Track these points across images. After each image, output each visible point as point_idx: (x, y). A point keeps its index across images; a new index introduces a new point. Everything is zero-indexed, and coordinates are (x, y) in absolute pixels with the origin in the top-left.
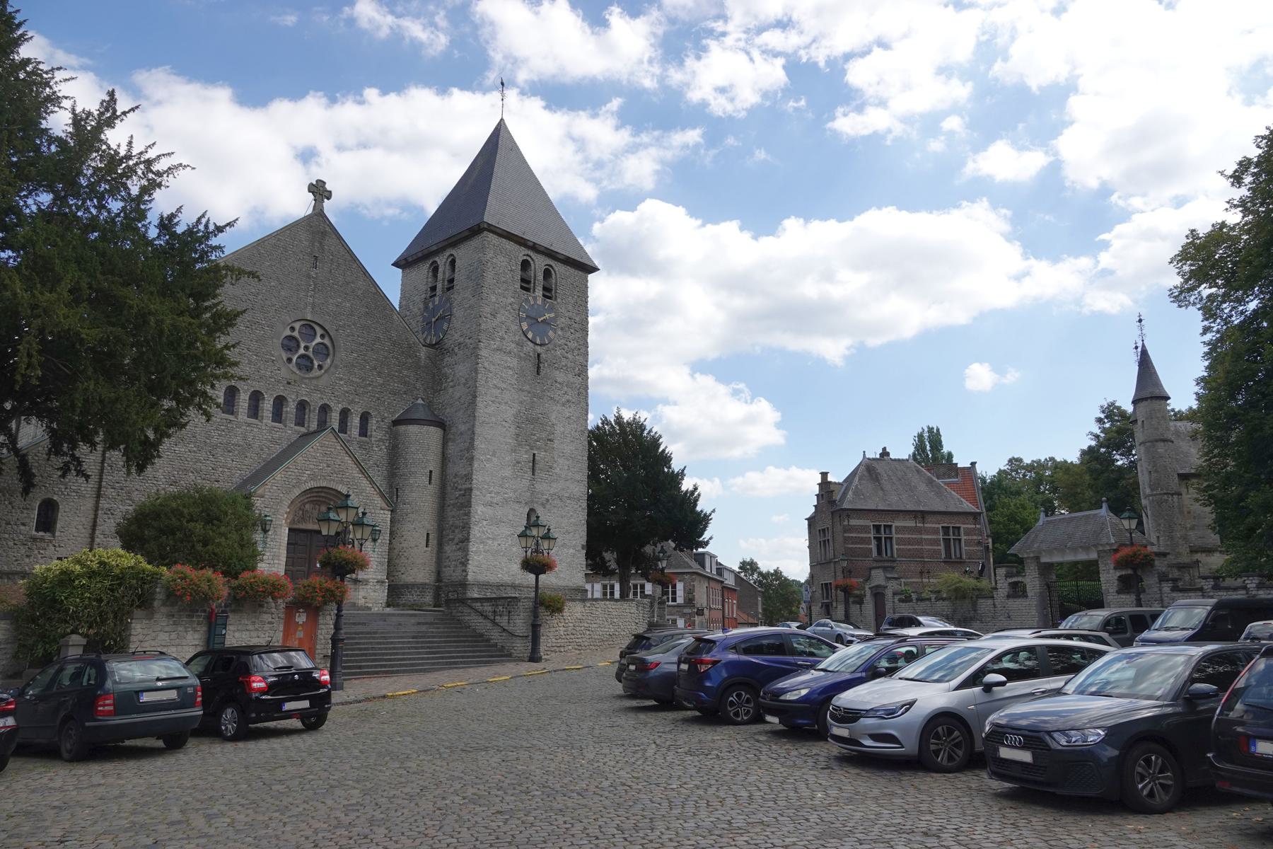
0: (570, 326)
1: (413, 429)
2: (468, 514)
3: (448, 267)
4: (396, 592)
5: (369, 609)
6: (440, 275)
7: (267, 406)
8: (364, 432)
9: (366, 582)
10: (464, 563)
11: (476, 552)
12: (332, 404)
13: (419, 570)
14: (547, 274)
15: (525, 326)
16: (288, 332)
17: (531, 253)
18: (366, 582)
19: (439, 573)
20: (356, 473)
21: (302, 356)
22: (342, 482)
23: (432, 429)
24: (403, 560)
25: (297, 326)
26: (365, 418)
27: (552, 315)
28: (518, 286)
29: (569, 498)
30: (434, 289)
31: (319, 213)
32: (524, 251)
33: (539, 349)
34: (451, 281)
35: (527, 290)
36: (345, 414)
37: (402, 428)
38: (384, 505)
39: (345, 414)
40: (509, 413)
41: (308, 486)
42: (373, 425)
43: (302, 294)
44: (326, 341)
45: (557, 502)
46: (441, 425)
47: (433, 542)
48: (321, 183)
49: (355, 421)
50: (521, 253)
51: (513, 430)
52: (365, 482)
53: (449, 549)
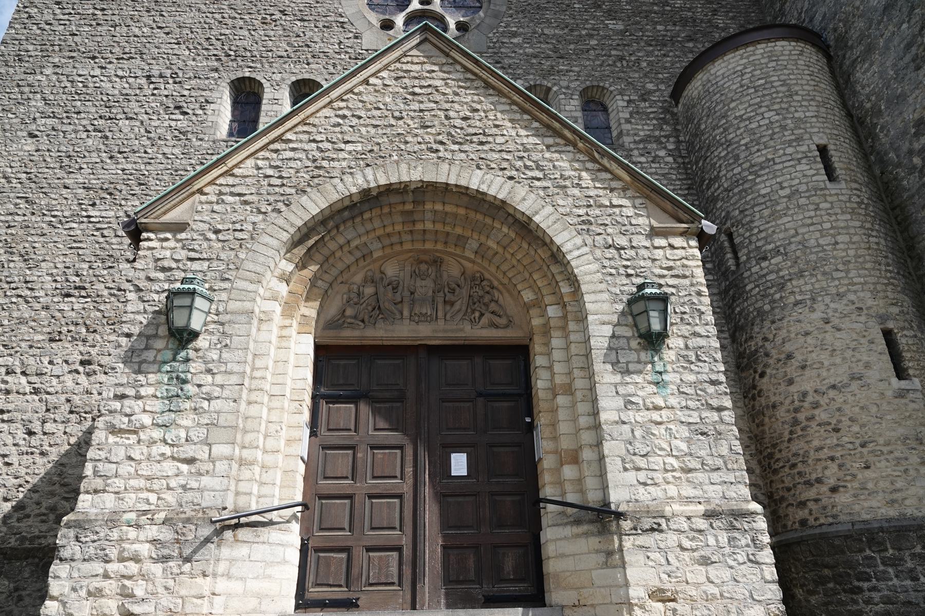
1: (724, 67)
9: (654, 523)
24: (817, 437)
37: (695, 87)
41: (354, 184)
42: (619, 107)
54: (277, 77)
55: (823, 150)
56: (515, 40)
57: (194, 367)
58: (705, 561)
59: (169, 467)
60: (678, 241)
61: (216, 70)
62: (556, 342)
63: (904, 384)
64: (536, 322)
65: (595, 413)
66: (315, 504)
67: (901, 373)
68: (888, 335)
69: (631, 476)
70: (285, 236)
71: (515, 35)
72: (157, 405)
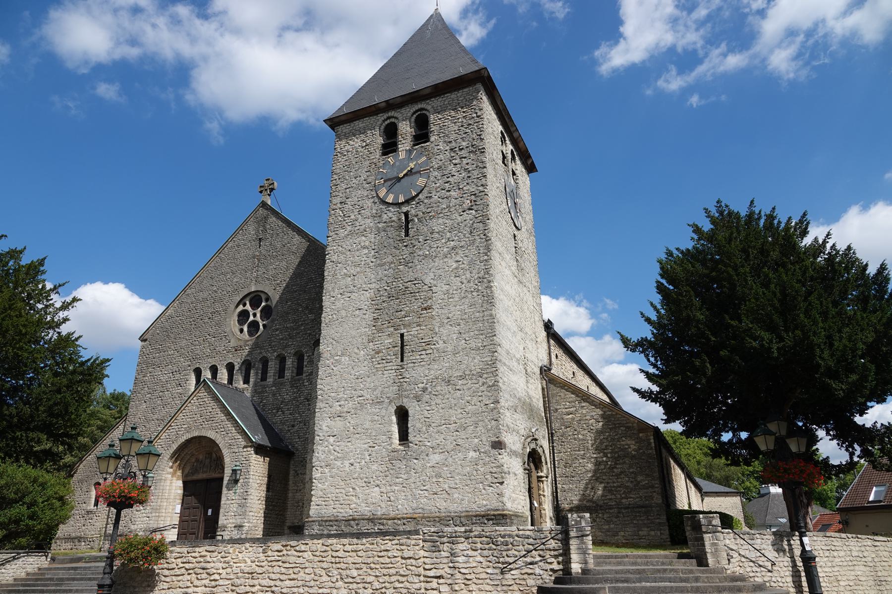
16: (241, 308)
22: (211, 428)
27: (424, 158)
29: (462, 377)
32: (382, 117)
33: (405, 209)
36: (282, 360)
39: (282, 360)
40: (364, 298)
43: (248, 274)
45: (441, 388)
51: (369, 316)
60: (249, 449)
66: (179, 525)
71: (277, 330)
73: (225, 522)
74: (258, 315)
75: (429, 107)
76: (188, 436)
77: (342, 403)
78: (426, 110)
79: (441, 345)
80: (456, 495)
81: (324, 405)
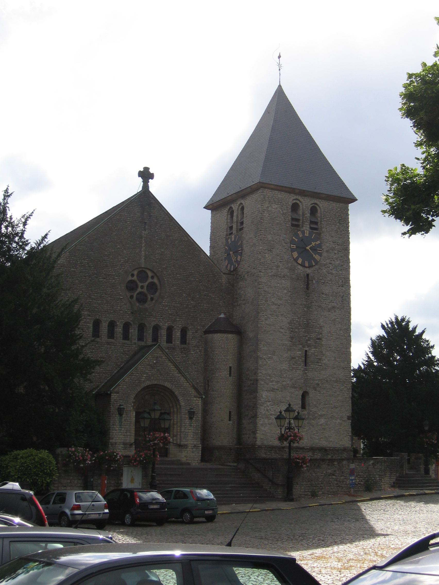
0: (333, 249)
2: (255, 398)
3: (240, 212)
4: (207, 452)
5: (189, 464)
6: (235, 218)
7: (119, 330)
8: (184, 340)
10: (254, 433)
11: (262, 425)
12: (161, 324)
13: (224, 436)
14: (314, 210)
15: (295, 255)
16: (130, 278)
17: (299, 198)
18: (186, 446)
19: (239, 439)
20: (176, 374)
21: (140, 293)
23: (230, 336)
25: (135, 273)
26: (184, 332)
27: (318, 242)
28: (289, 224)
30: (231, 228)
31: (145, 191)
33: (308, 271)
34: (242, 223)
35: (297, 226)
36: (170, 330)
38: (196, 394)
39: (170, 330)
42: (190, 334)
44: (155, 280)
46: (238, 331)
47: (234, 417)
48: (146, 169)
49: (177, 334)
50: (291, 199)
52: (182, 379)
53: (245, 422)
54: (105, 319)
55: (230, 367)
56: (167, 308)
57: (123, 420)
58: (193, 453)
59: (121, 436)
61: (90, 316)
62: (175, 416)
63: (230, 422)
64: (172, 410)
65: (181, 430)
67: (230, 420)
68: (230, 412)
69: (184, 440)
70: (134, 395)
72: (118, 426)
73: (186, 443)
74: (145, 288)
75: (321, 206)
76: (148, 383)
77: (274, 383)
78: (318, 205)
79: (326, 361)
80: (331, 440)
81: (263, 383)
